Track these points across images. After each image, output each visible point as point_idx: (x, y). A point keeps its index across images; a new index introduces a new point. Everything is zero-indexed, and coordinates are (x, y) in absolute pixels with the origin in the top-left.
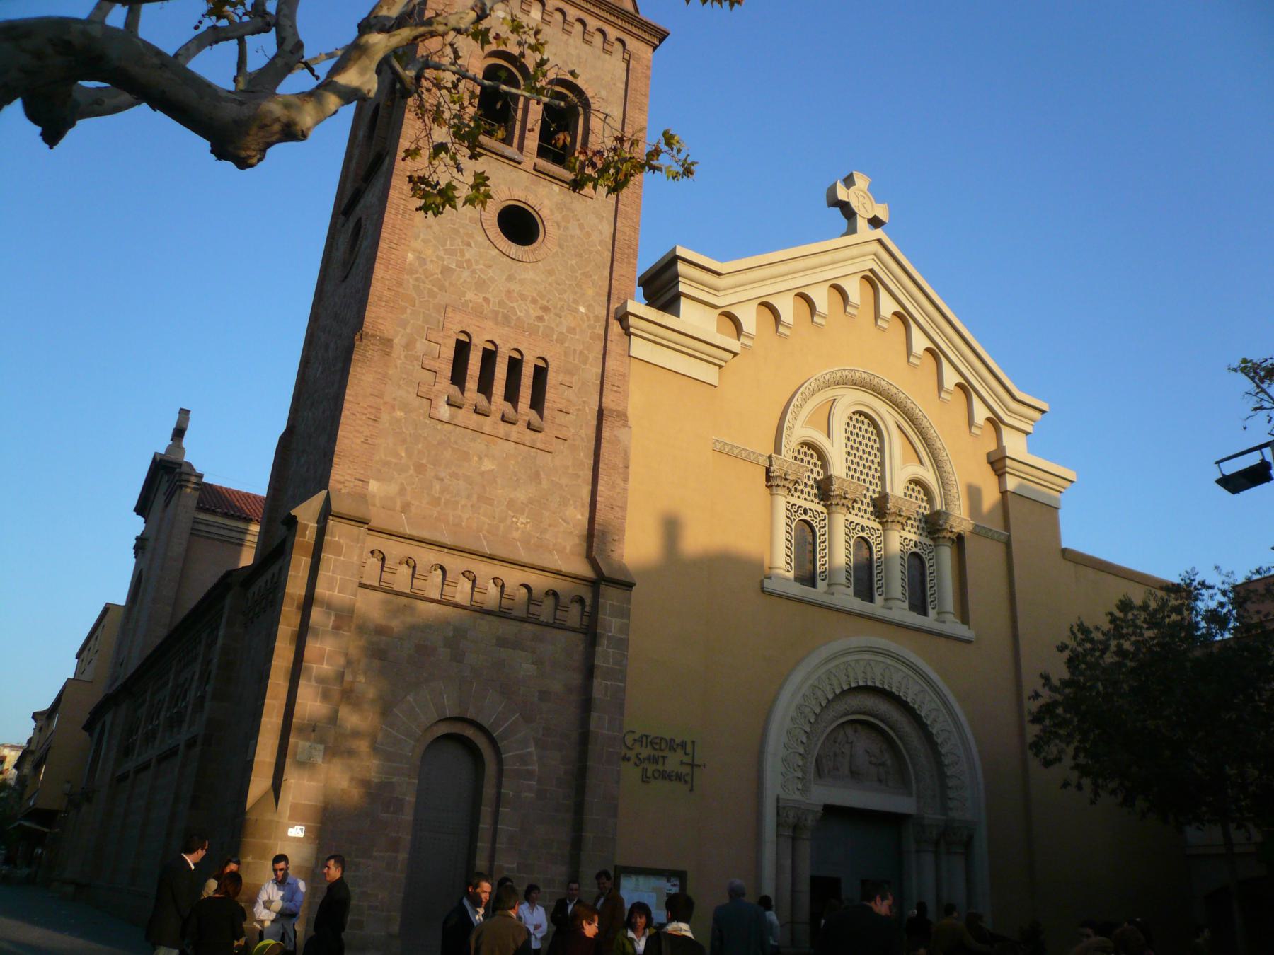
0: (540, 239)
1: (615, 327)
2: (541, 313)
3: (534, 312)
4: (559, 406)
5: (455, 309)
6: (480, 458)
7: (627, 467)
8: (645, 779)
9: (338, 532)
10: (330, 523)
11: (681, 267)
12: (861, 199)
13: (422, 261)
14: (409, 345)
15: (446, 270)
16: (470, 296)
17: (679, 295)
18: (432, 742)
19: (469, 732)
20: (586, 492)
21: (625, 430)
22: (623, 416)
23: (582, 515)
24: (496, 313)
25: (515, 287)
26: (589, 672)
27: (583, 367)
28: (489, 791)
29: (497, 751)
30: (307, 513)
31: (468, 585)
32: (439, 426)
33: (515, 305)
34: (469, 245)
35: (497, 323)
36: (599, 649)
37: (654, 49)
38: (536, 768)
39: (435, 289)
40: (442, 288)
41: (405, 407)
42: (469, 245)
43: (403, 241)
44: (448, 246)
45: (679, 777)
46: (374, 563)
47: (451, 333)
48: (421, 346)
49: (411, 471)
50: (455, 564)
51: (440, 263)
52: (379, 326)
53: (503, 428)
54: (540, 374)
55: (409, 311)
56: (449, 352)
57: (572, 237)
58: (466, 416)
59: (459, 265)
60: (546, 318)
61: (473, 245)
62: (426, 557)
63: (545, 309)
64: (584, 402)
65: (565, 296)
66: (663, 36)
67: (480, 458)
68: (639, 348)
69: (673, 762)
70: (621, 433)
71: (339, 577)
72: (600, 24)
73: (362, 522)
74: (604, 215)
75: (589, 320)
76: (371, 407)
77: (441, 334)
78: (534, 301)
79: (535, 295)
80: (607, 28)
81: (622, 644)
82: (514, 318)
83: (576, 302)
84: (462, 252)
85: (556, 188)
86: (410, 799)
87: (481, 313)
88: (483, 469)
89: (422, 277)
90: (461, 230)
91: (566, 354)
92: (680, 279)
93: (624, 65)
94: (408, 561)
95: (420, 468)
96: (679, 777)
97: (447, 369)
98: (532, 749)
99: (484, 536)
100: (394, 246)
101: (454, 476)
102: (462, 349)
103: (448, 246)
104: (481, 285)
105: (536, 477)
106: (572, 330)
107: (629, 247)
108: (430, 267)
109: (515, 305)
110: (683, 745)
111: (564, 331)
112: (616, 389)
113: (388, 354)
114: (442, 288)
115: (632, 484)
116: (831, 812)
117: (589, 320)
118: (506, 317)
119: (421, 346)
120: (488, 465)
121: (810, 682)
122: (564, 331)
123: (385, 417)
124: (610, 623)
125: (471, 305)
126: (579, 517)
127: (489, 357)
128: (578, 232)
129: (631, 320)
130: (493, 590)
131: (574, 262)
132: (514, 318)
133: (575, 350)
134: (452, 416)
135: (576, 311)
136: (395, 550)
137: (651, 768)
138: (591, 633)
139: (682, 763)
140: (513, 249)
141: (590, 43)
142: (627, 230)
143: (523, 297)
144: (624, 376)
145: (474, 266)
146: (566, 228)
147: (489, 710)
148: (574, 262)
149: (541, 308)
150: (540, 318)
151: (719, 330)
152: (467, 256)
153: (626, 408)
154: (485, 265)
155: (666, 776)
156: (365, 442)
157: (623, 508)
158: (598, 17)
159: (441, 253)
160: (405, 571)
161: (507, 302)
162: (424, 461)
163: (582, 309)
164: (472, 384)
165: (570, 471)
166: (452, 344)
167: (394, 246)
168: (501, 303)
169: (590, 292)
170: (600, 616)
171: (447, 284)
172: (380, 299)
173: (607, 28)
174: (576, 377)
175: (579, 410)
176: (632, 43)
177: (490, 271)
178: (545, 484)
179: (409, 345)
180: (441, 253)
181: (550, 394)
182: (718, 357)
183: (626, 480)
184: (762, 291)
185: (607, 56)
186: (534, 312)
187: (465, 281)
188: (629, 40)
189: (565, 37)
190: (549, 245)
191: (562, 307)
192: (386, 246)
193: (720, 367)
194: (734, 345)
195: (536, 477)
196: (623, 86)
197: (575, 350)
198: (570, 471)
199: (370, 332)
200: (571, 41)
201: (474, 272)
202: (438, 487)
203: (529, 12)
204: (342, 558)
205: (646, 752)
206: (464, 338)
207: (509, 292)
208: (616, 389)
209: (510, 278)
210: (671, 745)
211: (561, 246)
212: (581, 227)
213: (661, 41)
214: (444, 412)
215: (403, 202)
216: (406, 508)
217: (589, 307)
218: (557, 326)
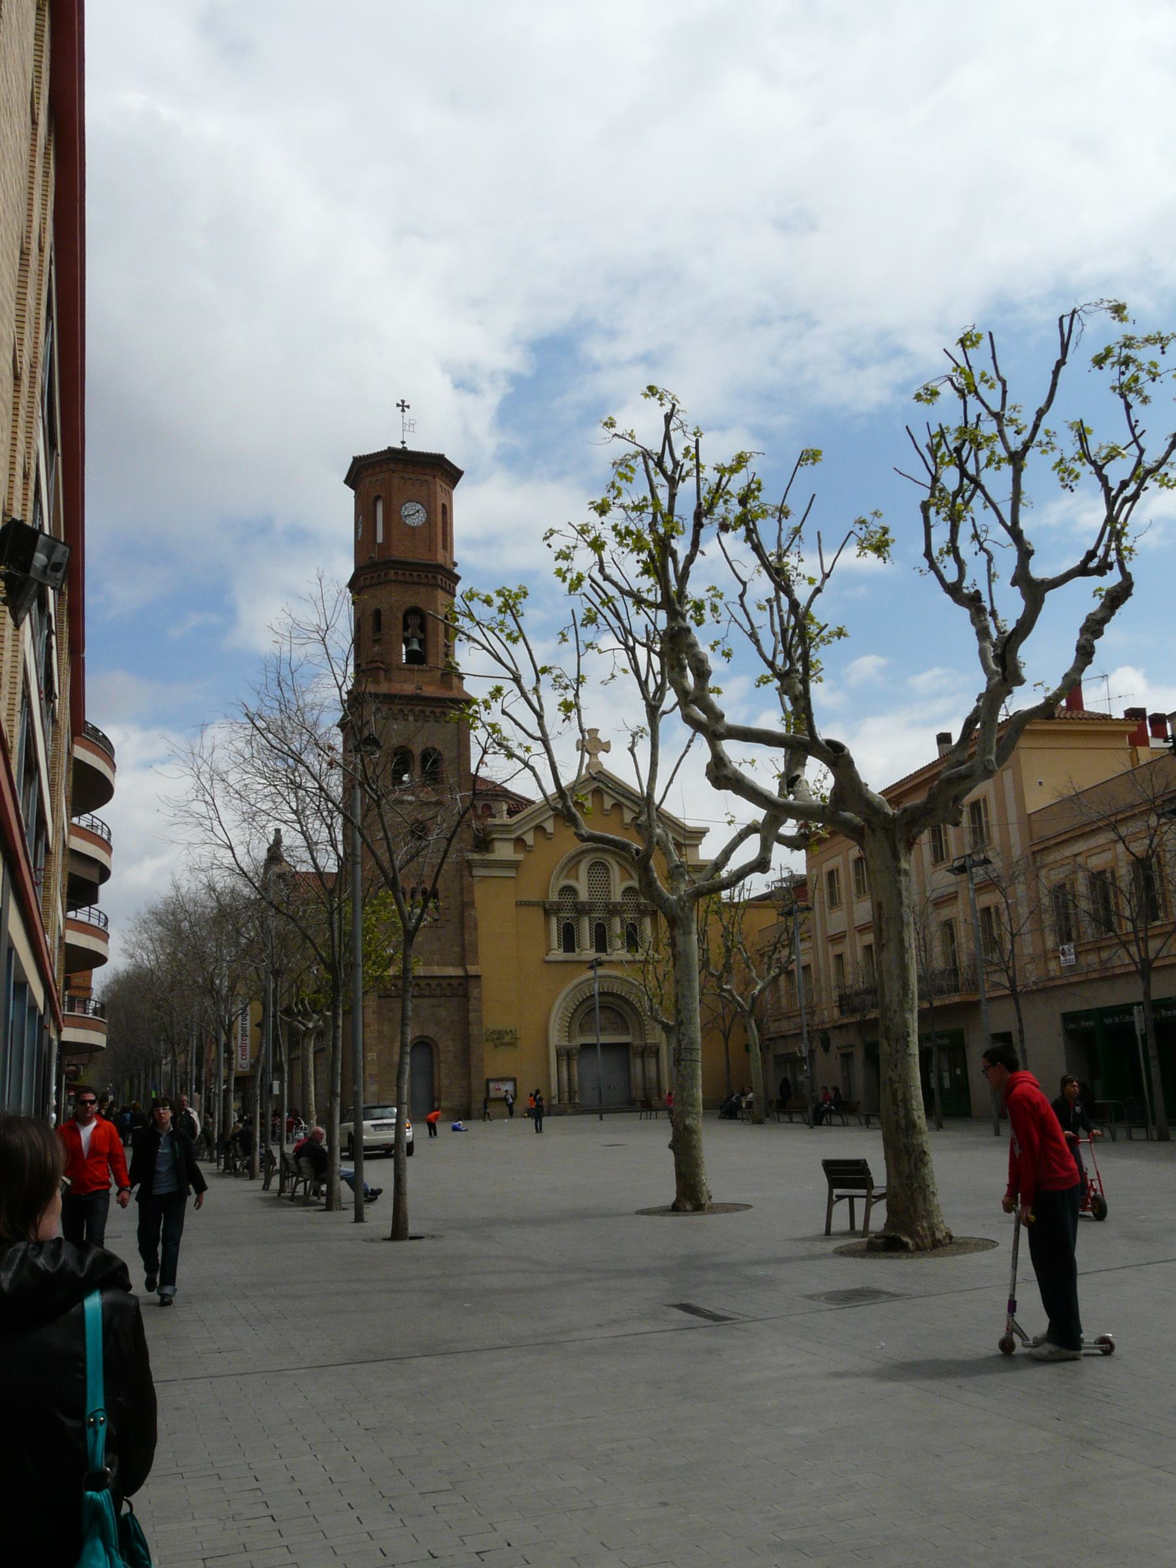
7: (476, 925)
19: (426, 1040)
22: (472, 904)
38: (451, 1048)
45: (511, 1044)
69: (507, 1039)
81: (479, 999)
96: (511, 1044)
98: (450, 1042)
137: (498, 1042)
144: (472, 886)
147: (430, 1031)
151: (515, 851)
158: (438, 707)
182: (514, 865)
183: (476, 930)
184: (534, 824)
194: (520, 857)
200: (429, 724)
205: (495, 1037)
210: (506, 1033)
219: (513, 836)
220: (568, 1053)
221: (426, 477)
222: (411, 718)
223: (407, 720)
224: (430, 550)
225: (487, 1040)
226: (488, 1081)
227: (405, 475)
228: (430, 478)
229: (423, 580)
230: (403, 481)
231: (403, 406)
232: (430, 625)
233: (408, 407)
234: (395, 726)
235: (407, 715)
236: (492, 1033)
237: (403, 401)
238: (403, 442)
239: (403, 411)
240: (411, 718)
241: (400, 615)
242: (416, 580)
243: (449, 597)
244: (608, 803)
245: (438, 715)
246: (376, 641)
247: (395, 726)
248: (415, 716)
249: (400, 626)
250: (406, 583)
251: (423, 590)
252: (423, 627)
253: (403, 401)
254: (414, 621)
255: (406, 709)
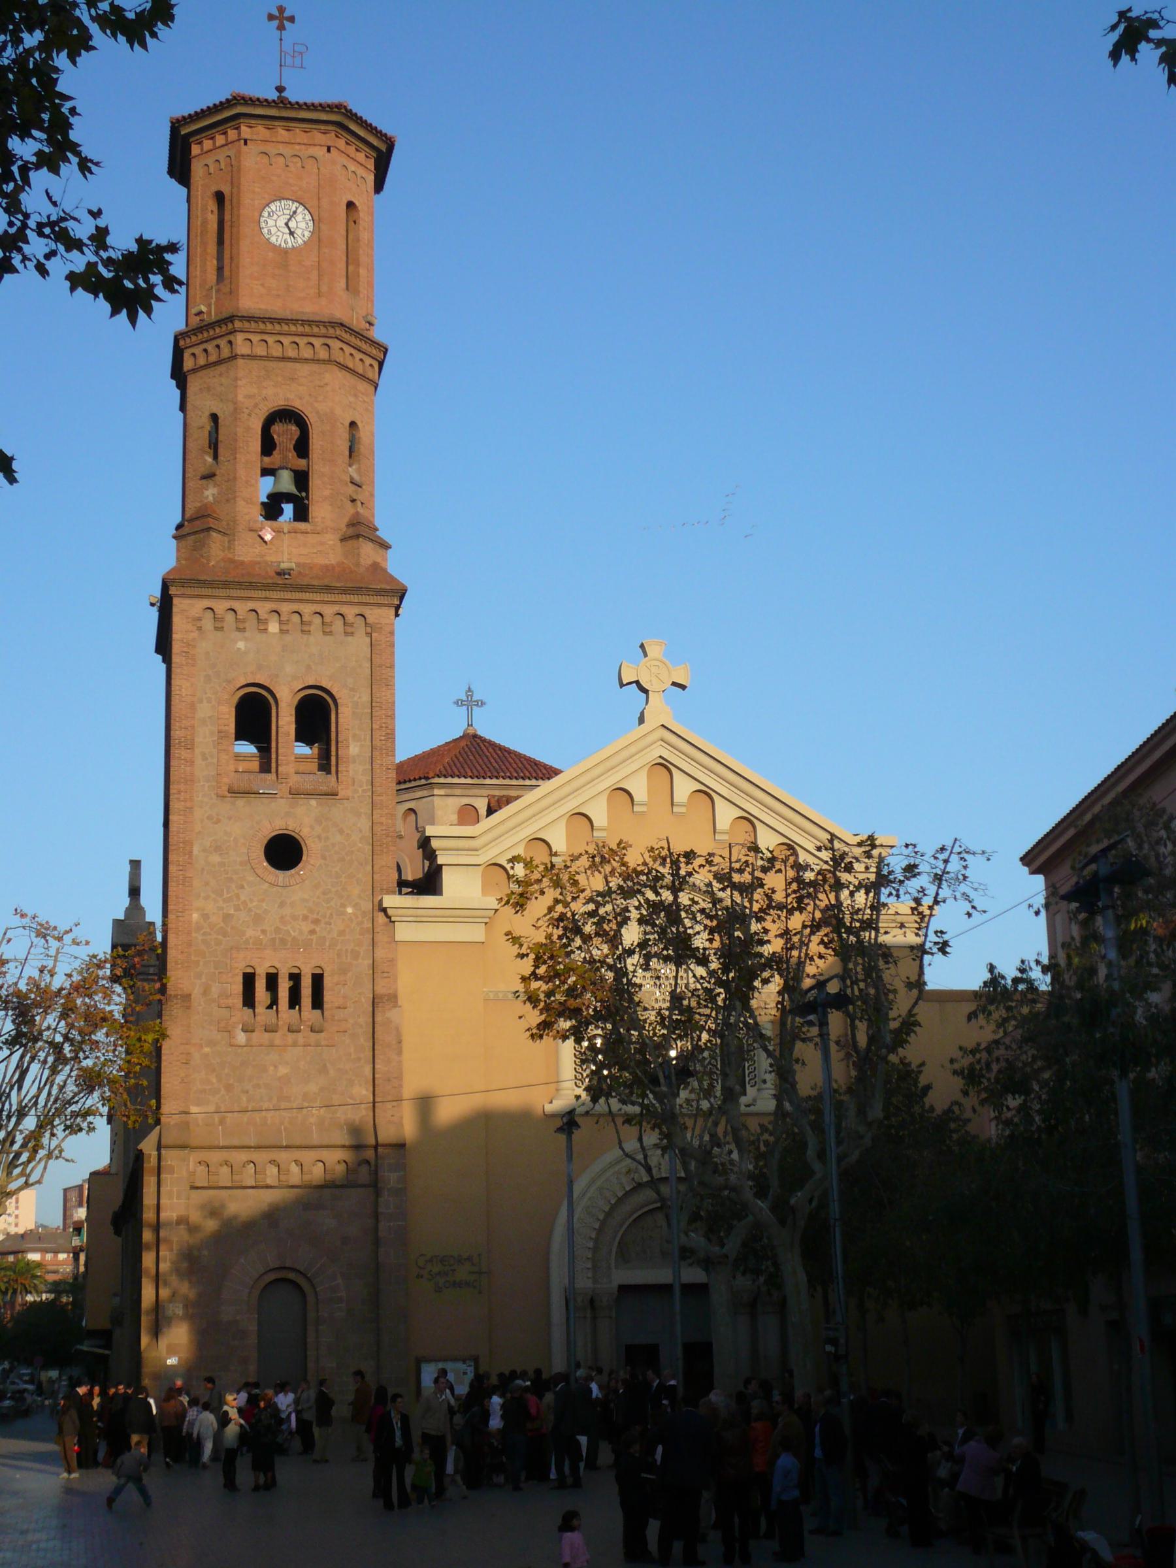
0: (304, 858)
1: (381, 917)
2: (313, 927)
3: (306, 927)
4: (336, 1005)
5: (238, 949)
6: (276, 1067)
8: (438, 1290)
9: (171, 1158)
10: (163, 1152)
11: (435, 844)
12: (654, 670)
13: (205, 916)
14: (206, 992)
15: (227, 918)
16: (250, 933)
17: (441, 866)
18: (265, 1287)
19: (291, 1276)
20: (368, 1070)
21: (395, 1011)
22: (393, 998)
23: (367, 1090)
24: (273, 940)
25: (287, 911)
26: (376, 1216)
27: (355, 962)
28: (311, 1315)
29: (313, 1285)
30: (148, 1146)
31: (275, 1170)
32: (240, 1050)
33: (289, 927)
34: (242, 887)
35: (275, 950)
36: (381, 1200)
37: (398, 608)
39: (220, 937)
40: (225, 934)
41: (211, 1043)
42: (242, 887)
43: (187, 907)
44: (226, 896)
46: (203, 1168)
47: (238, 971)
48: (215, 990)
49: (223, 1092)
50: (261, 1157)
51: (221, 912)
52: (181, 986)
53: (291, 1037)
54: (318, 980)
55: (201, 963)
56: (239, 988)
57: (333, 845)
58: (259, 1036)
59: (237, 909)
60: (318, 929)
61: (246, 886)
62: (241, 1157)
63: (316, 922)
64: (360, 994)
65: (332, 903)
66: (402, 594)
67: (276, 1067)
68: (404, 932)
70: (392, 1014)
71: (175, 1189)
72: (336, 608)
73: (183, 1147)
74: (362, 811)
75: (357, 917)
76: (182, 1053)
77: (230, 975)
78: (305, 918)
79: (305, 912)
80: (344, 609)
82: (290, 939)
83: (344, 906)
84: (238, 896)
85: (313, 802)
86: (253, 1327)
87: (261, 944)
88: (279, 1074)
89: (208, 930)
90: (234, 877)
91: (339, 955)
92: (437, 853)
93: (368, 640)
94: (226, 1163)
95: (229, 1088)
97: (239, 1001)
98: (340, 1281)
99: (285, 1129)
100: (180, 914)
101: (258, 1086)
102: (249, 980)
103: (226, 896)
104: (258, 919)
105: (323, 1070)
106: (341, 933)
107: (388, 836)
108: (213, 919)
109: (289, 927)
110: (469, 1259)
111: (335, 936)
112: (385, 975)
113: (189, 1008)
114: (225, 934)
115: (407, 1055)
116: (624, 1289)
117: (357, 917)
118: (283, 942)
119: (215, 990)
120: (283, 1070)
121: (598, 1183)
122: (335, 936)
123: (196, 1056)
124: (391, 1178)
125: (251, 941)
126: (364, 1092)
127: (272, 981)
128: (338, 838)
129: (390, 912)
130: (295, 1169)
131: (337, 869)
132: (290, 939)
133: (347, 950)
134: (248, 1040)
135: (344, 913)
136: (215, 1157)
138: (375, 1185)
139: (470, 1273)
140: (281, 876)
141: (330, 633)
142: (383, 820)
143: (295, 918)
144: (392, 961)
145: (250, 905)
146: (327, 838)
148: (337, 869)
149: (312, 922)
150: (312, 932)
152: (243, 898)
153: (396, 991)
154: (259, 901)
155: (456, 1285)
156: (182, 1081)
157: (400, 1078)
159: (221, 904)
160: (225, 1170)
161: (282, 927)
162: (231, 1082)
163: (350, 910)
164: (260, 1008)
165: (353, 1056)
166: (240, 979)
167: (180, 914)
168: (277, 930)
169: (356, 891)
170: (380, 1174)
171: (229, 929)
172: (176, 963)
173: (344, 609)
174: (350, 974)
175: (356, 1002)
176: (373, 614)
177: (264, 905)
178: (332, 1072)
179: (206, 992)
180: (221, 904)
181: (328, 997)
185: (350, 639)
186: (306, 927)
187: (244, 922)
188: (367, 611)
189: (305, 637)
190: (312, 862)
191: (331, 914)
192: (174, 917)
193: (486, 923)
195: (323, 1070)
196: (368, 665)
197: (347, 950)
198: (353, 1056)
199: (173, 993)
200: (312, 639)
201: (250, 910)
202: (244, 1099)
203: (266, 629)
204: (175, 1175)
206: (250, 970)
207: (282, 917)
208: (385, 975)
209: (282, 905)
211: (324, 858)
212: (341, 832)
213: (402, 598)
214: (241, 1038)
215: (181, 873)
216: (222, 1122)
217: (356, 906)
218: (329, 932)
219: (484, 858)
220: (592, 1301)
221: (313, 151)
222: (274, 627)
223: (265, 631)
224: (319, 295)
225: (420, 1276)
226: (419, 1362)
227: (272, 149)
228: (320, 152)
229: (307, 353)
230: (265, 159)
231: (281, 18)
232: (316, 443)
233: (292, 19)
234: (241, 645)
235: (266, 622)
236: (431, 1260)
237: (281, 9)
238: (280, 89)
239: (281, 28)
240: (274, 627)
241: (257, 426)
242: (291, 353)
243: (363, 386)
244: (684, 788)
245: (327, 619)
246: (209, 476)
247: (241, 645)
248: (281, 622)
249: (256, 445)
250: (268, 358)
251: (303, 370)
252: (302, 447)
253: (281, 9)
254: (285, 434)
255: (264, 608)
